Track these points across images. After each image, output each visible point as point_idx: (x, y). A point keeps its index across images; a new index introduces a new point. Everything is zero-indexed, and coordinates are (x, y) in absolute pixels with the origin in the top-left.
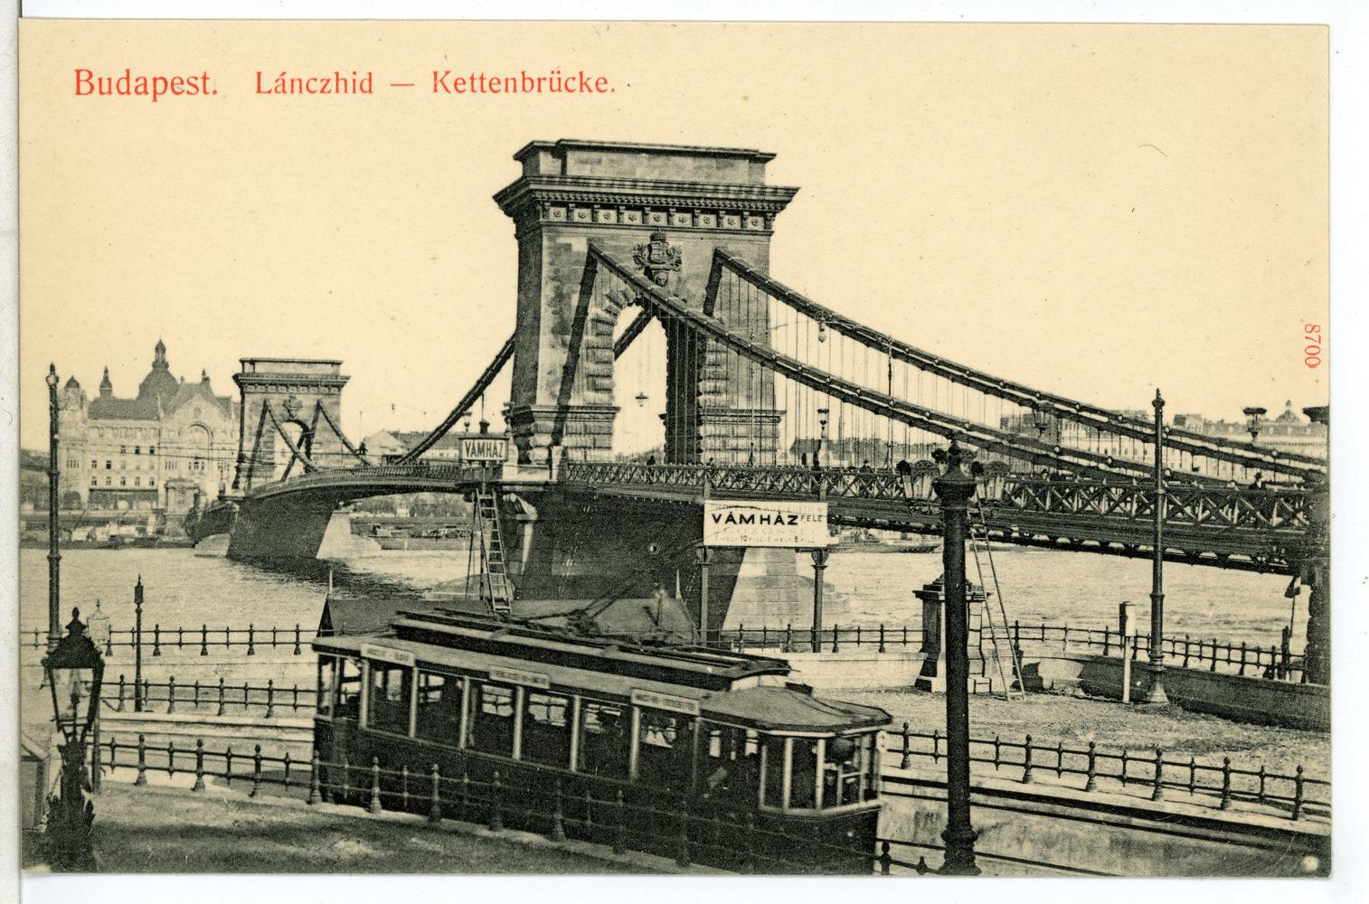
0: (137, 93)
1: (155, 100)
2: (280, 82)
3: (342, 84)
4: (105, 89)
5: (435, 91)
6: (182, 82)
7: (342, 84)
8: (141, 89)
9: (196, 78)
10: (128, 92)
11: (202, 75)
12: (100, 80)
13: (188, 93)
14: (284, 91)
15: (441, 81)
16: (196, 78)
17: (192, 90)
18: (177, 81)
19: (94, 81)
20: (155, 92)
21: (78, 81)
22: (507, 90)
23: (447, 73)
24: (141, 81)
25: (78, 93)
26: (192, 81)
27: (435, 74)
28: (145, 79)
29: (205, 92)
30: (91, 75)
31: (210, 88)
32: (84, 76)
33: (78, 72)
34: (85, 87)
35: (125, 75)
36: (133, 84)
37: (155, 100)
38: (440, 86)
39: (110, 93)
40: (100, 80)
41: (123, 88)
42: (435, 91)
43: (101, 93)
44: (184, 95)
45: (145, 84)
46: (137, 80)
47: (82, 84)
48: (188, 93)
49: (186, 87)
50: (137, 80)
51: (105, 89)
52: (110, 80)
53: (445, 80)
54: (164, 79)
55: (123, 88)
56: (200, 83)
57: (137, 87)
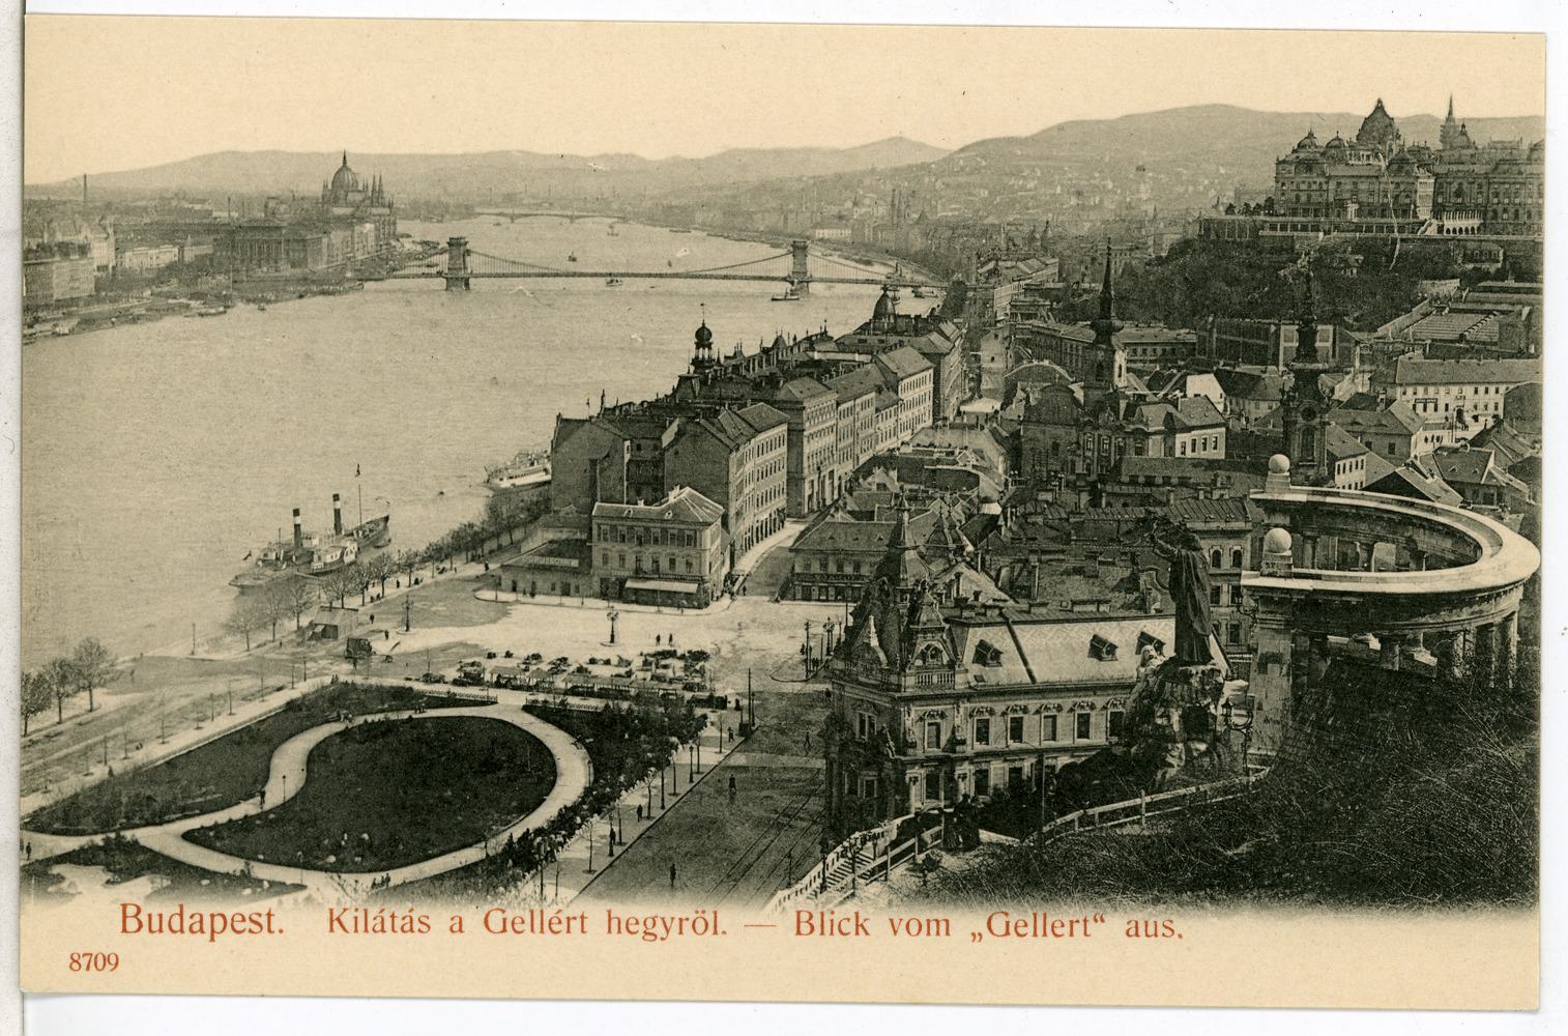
0: (192, 931)
1: (212, 939)
2: (379, 919)
3: (614, 923)
4: (155, 926)
5: (332, 930)
6: (244, 920)
7: (614, 923)
8: (196, 927)
9: (260, 915)
10: (182, 931)
11: (264, 912)
12: (150, 916)
13: (250, 931)
14: (383, 930)
15: (338, 919)
16: (260, 915)
17: (256, 928)
18: (239, 918)
19: (143, 917)
20: (213, 931)
21: (125, 917)
22: (1035, 934)
23: (345, 910)
24: (197, 918)
25: (124, 930)
26: (255, 917)
27: (331, 911)
28: (201, 916)
29: (270, 931)
30: (139, 910)
31: (272, 929)
32: (131, 911)
33: (124, 906)
34: (132, 924)
35: (178, 911)
36: (187, 923)
37: (212, 939)
38: (336, 924)
39: (161, 931)
40: (150, 916)
41: (176, 926)
42: (332, 930)
43: (151, 931)
44: (247, 932)
45: (201, 922)
46: (192, 917)
47: (128, 920)
48: (250, 931)
49: (248, 925)
50: (192, 917)
51: (155, 926)
52: (161, 916)
53: (342, 918)
54: (223, 916)
55: (176, 926)
56: (263, 920)
57: (191, 927)
